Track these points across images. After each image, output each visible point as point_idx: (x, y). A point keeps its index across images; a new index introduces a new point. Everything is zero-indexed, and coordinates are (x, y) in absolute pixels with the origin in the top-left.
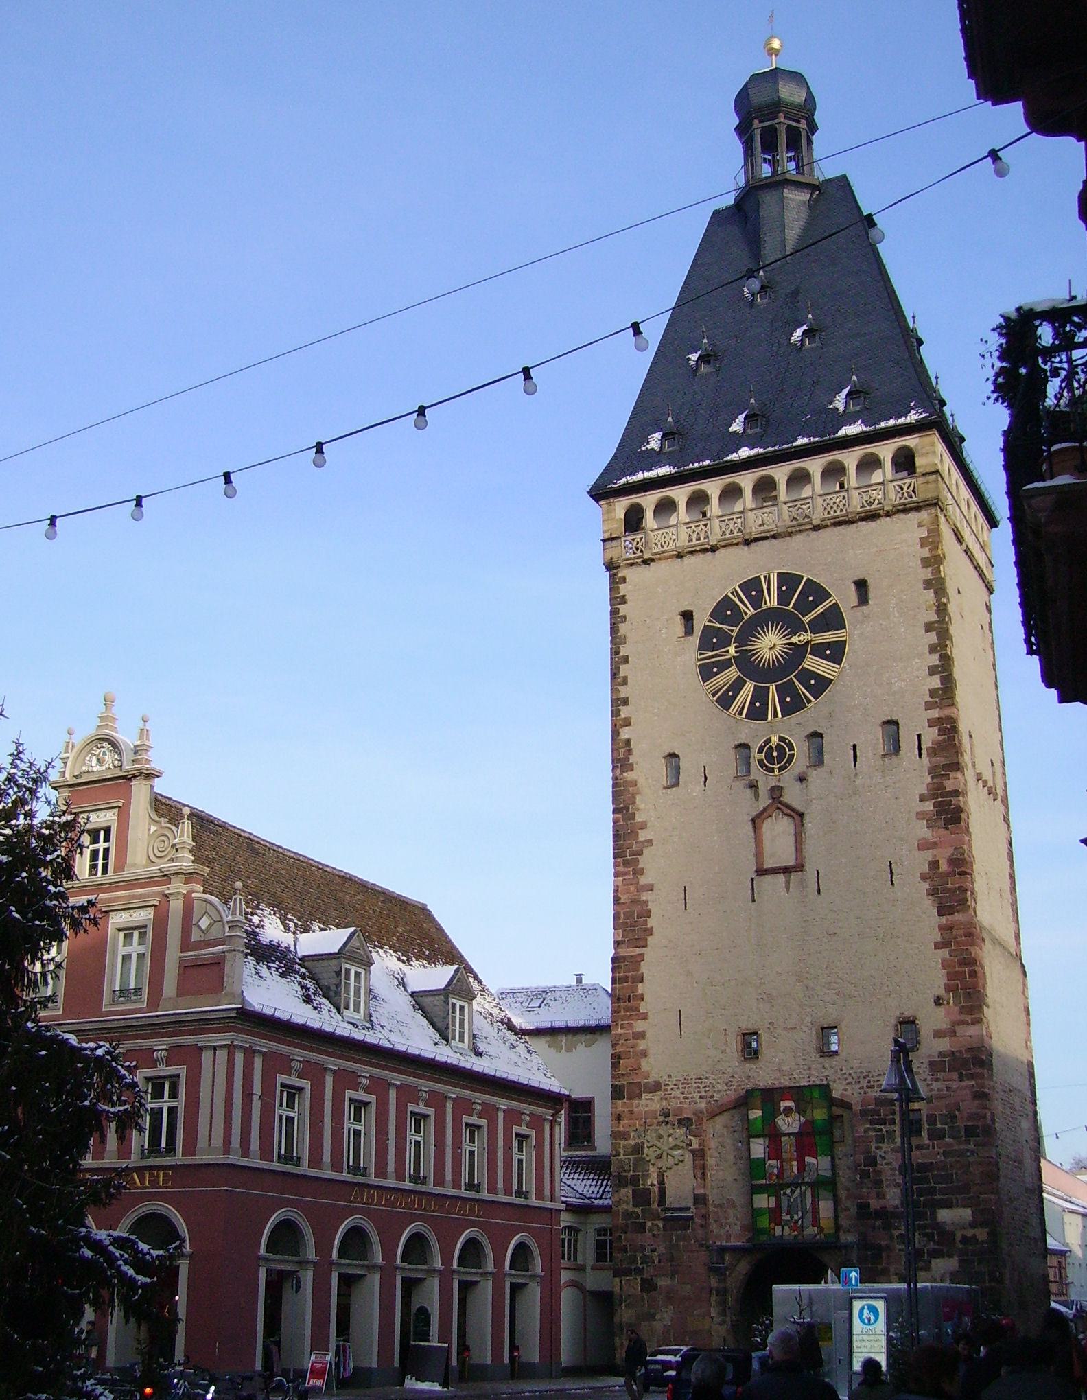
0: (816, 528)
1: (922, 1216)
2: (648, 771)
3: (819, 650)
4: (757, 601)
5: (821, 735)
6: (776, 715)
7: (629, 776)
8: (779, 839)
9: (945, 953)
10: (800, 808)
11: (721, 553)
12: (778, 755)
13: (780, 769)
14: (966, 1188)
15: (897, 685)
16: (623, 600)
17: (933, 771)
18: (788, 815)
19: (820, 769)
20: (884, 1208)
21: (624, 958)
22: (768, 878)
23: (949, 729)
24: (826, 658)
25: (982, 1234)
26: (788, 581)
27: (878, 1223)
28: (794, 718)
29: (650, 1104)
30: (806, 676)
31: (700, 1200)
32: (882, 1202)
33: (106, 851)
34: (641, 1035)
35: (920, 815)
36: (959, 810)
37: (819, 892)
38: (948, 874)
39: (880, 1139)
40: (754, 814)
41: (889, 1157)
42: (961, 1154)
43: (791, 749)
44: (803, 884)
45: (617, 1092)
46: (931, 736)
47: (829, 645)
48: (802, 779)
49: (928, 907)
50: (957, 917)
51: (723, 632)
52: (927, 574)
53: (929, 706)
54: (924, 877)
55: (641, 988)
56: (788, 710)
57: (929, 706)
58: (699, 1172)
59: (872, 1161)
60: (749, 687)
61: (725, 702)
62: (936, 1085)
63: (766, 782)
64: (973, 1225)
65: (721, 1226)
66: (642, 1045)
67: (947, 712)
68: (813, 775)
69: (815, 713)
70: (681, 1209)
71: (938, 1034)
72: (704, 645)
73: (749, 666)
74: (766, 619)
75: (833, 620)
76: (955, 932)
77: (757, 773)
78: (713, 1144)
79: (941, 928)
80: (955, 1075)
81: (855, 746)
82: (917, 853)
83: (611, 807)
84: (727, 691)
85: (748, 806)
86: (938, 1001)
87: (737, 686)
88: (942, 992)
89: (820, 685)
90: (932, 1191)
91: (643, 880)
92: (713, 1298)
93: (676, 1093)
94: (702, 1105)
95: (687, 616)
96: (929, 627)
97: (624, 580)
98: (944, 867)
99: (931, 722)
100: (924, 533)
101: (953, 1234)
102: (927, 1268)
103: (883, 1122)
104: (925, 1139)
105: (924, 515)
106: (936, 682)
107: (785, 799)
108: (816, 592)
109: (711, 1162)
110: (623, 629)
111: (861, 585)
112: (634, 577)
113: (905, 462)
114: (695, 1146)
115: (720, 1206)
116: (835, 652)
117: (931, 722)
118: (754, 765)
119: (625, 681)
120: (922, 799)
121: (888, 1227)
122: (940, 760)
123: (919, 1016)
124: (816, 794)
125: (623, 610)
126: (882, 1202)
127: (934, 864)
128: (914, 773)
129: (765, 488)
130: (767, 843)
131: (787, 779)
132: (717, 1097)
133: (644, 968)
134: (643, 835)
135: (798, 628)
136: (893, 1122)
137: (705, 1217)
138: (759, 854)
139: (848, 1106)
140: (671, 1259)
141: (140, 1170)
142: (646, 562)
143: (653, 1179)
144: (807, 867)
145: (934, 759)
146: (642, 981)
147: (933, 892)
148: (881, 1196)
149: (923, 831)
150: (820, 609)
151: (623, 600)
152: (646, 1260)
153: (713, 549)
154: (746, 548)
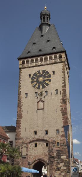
0: (48, 64)
1: (59, 157)
2: (23, 95)
3: (47, 80)
4: (39, 73)
5: (47, 91)
7: (20, 96)
9: (63, 121)
10: (44, 101)
12: (41, 94)
14: (65, 153)
15: (58, 85)
16: (21, 73)
17: (62, 96)
18: (42, 102)
19: (47, 96)
20: (54, 156)
21: (18, 120)
22: (39, 110)
23: (65, 91)
25: (67, 160)
26: (44, 71)
27: (53, 158)
28: (44, 89)
29: (21, 141)
30: (46, 83)
31: (27, 155)
32: (53, 155)
34: (20, 131)
35: (60, 102)
38: (64, 110)
39: (53, 146)
41: (54, 149)
42: (65, 148)
44: (44, 111)
45: (16, 139)
46: (62, 92)
47: (49, 79)
48: (44, 97)
49: (61, 114)
50: (65, 116)
51: (34, 78)
52: (63, 71)
53: (62, 88)
54: (61, 110)
55: (20, 125)
56: (43, 88)
57: (62, 88)
59: (52, 149)
60: (38, 85)
61: (34, 86)
62: (61, 139)
63: (39, 97)
64: (66, 159)
66: (20, 133)
67: (65, 89)
69: (47, 88)
70: (24, 156)
71: (62, 132)
72: (32, 79)
73: (37, 81)
74: (40, 76)
75: (50, 76)
76: (65, 118)
77: (38, 96)
79: (63, 117)
80: (64, 138)
83: (18, 100)
86: (62, 127)
87: (36, 84)
88: (63, 126)
89: (48, 85)
90: (61, 154)
91: (21, 110)
93: (24, 139)
94: (28, 141)
95: (30, 75)
96: (63, 78)
97: (21, 70)
98: (63, 109)
99: (62, 90)
100: (62, 65)
101: (63, 160)
102: (59, 165)
103: (54, 144)
104: (60, 146)
105: (63, 63)
106: (63, 85)
108: (48, 72)
109: (29, 149)
110: (21, 77)
111: (54, 72)
112: (23, 70)
113: (60, 57)
114: (27, 147)
116: (50, 80)
118: (38, 95)
119: (21, 83)
121: (54, 159)
123: (59, 129)
124: (46, 99)
125: (21, 74)
126: (53, 155)
127: (62, 109)
128: (60, 97)
131: (42, 97)
133: (21, 122)
134: (22, 104)
135: (45, 77)
136: (55, 144)
137: (28, 157)
139: (49, 142)
140: (23, 163)
143: (21, 151)
146: (20, 123)
147: (62, 112)
148: (53, 154)
149: (61, 104)
150: (48, 75)
151: (21, 73)
152: (19, 163)
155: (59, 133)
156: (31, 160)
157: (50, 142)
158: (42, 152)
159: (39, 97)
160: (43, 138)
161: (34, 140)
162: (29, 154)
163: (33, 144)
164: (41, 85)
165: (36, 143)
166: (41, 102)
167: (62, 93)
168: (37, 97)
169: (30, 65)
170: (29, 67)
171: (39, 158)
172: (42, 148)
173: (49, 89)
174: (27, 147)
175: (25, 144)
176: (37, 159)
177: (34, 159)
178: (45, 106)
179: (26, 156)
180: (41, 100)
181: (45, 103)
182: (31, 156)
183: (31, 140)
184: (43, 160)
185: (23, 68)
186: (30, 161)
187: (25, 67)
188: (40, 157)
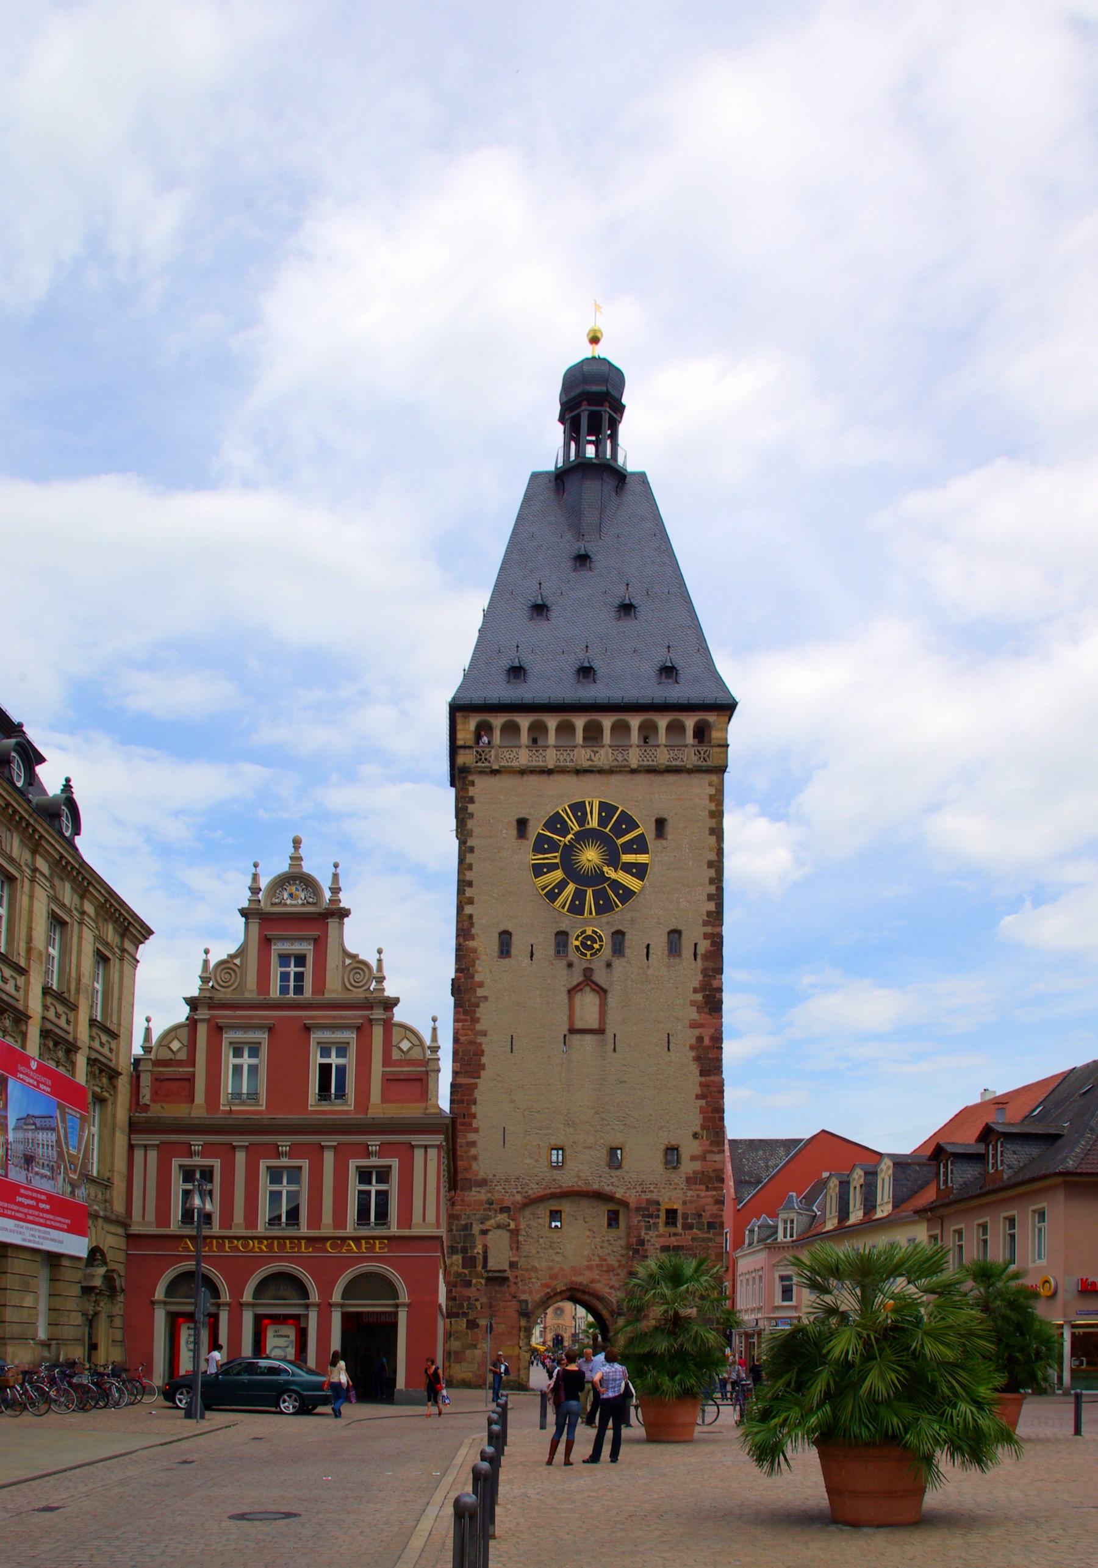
4: (582, 821)
6: (591, 913)
8: (588, 1007)
10: (604, 986)
11: (555, 778)
12: (588, 943)
13: (592, 955)
17: (704, 972)
18: (594, 990)
19: (622, 959)
22: (578, 1036)
24: (633, 875)
28: (605, 918)
31: (513, 1265)
33: (299, 977)
35: (693, 1003)
36: (721, 1002)
37: (614, 1050)
38: (709, 1047)
40: (570, 986)
43: (601, 940)
44: (603, 1043)
46: (704, 946)
48: (609, 965)
49: (694, 1069)
51: (554, 842)
53: (705, 924)
54: (692, 1048)
57: (705, 924)
58: (515, 1246)
60: (571, 888)
65: (525, 1285)
67: (717, 930)
68: (617, 963)
69: (621, 916)
70: (499, 1271)
76: (712, 1089)
77: (573, 955)
78: (523, 1226)
81: (648, 945)
82: (689, 1031)
84: (554, 888)
85: (564, 979)
87: (562, 885)
89: (627, 894)
92: (522, 1334)
94: (518, 1198)
98: (707, 1041)
99: (706, 936)
107: (595, 978)
109: (521, 1238)
114: (512, 1226)
115: (526, 1270)
117: (706, 936)
120: (695, 991)
122: (711, 965)
124: (620, 977)
127: (700, 1039)
128: (690, 972)
129: (593, 733)
130: (577, 1010)
132: (530, 1192)
138: (571, 1017)
141: (357, 1240)
142: (494, 772)
144: (607, 1031)
145: (706, 963)
147: (697, 1059)
149: (693, 1014)
153: (550, 772)
154: (575, 777)
155: (678, 1162)
156: (531, 1293)
157: (633, 1205)
158: (586, 1253)
159: (580, 964)
160: (596, 1187)
161: (549, 1191)
162: (522, 1263)
163: (543, 1211)
164: (590, 892)
165: (554, 1205)
166: (588, 989)
167: (701, 950)
168: (565, 962)
169: (524, 758)
170: (523, 772)
171: (573, 1283)
172: (588, 1233)
173: (633, 920)
174: (512, 1226)
175: (504, 1210)
176: (561, 1287)
177: (546, 1285)
178: (612, 1017)
179: (508, 1274)
180: (588, 981)
181: (613, 1000)
182: (533, 1275)
183: (534, 1190)
184: (589, 1293)
185: (482, 772)
186: (523, 1297)
187: (496, 767)
188: (579, 1279)
